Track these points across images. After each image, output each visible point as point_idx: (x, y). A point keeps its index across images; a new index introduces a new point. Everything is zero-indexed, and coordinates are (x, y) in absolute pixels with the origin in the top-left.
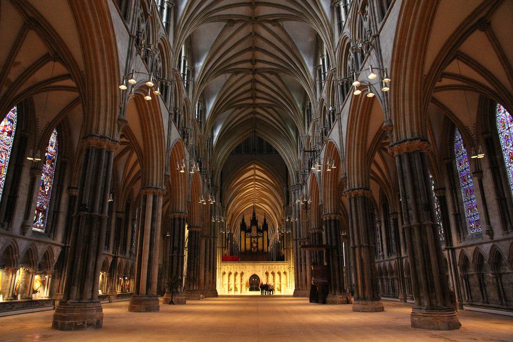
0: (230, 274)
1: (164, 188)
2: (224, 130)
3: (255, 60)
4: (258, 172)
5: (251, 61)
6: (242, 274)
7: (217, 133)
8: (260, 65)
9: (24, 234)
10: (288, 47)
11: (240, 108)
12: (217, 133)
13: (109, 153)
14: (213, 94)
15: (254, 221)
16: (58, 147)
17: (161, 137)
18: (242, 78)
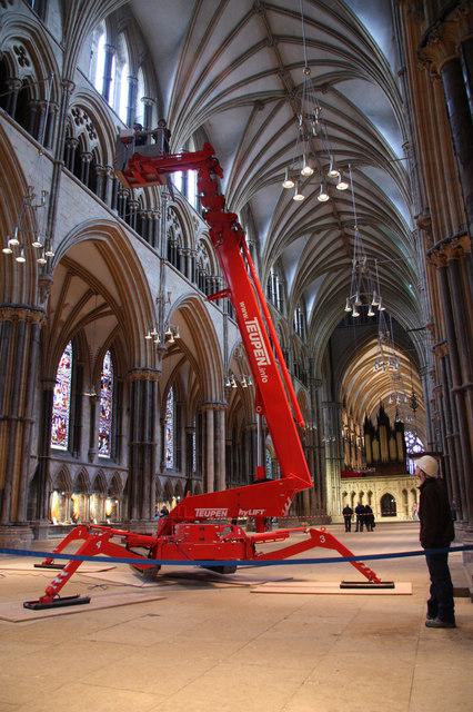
0: (354, 494)
1: (225, 402)
2: (319, 302)
3: (338, 213)
4: (385, 348)
5: (332, 214)
6: (370, 494)
7: (310, 308)
8: (345, 218)
9: (91, 460)
10: (372, 194)
11: (336, 271)
12: (310, 308)
13: (153, 383)
14: (293, 261)
15: (383, 418)
16: (113, 367)
17: (215, 345)
18: (327, 235)
